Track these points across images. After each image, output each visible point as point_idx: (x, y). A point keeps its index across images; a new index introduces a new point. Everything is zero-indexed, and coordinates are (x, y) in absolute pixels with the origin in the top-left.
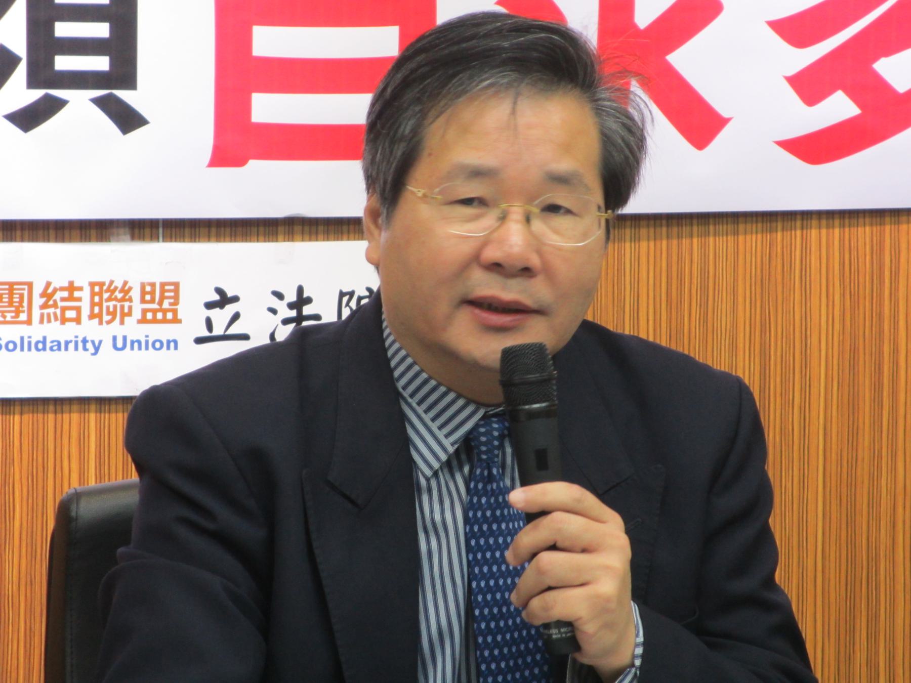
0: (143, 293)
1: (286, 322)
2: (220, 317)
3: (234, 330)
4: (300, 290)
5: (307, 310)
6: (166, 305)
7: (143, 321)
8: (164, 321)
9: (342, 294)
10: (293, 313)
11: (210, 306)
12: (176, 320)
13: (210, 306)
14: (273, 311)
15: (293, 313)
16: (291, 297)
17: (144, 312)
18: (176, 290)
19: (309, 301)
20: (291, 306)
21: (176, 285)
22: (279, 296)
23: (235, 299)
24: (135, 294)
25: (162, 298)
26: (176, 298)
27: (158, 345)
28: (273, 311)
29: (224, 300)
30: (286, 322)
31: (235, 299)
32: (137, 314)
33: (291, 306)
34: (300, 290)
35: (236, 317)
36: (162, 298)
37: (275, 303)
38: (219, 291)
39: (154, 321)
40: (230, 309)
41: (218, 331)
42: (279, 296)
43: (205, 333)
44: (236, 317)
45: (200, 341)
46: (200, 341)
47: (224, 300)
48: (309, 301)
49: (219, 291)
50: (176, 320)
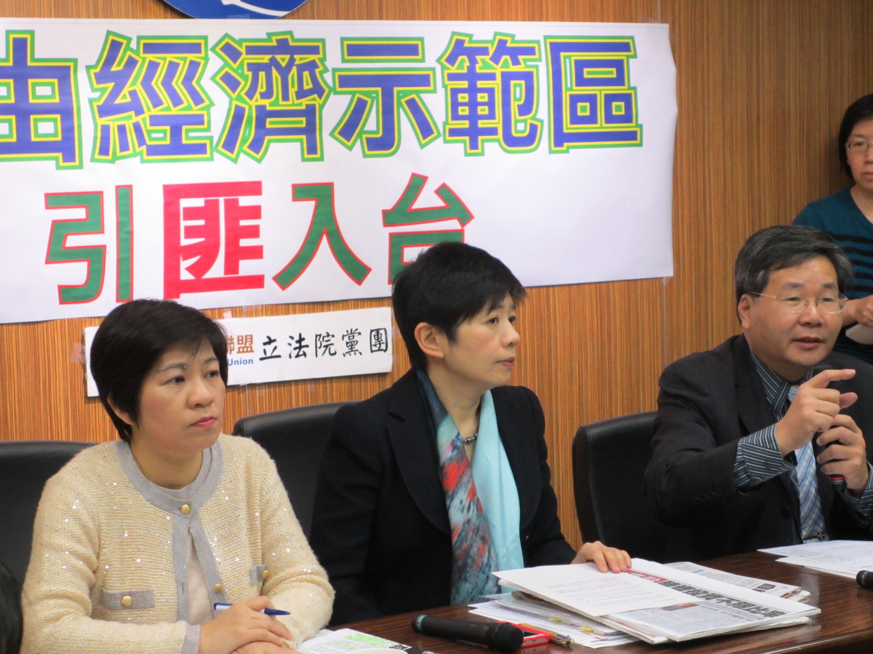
0: (239, 340)
1: (295, 349)
2: (269, 348)
3: (274, 354)
4: (300, 335)
5: (303, 343)
6: (248, 345)
7: (239, 352)
8: (247, 351)
9: (317, 336)
10: (298, 345)
11: (265, 344)
12: (252, 351)
13: (265, 344)
14: (290, 345)
15: (298, 345)
16: (297, 338)
17: (239, 348)
18: (251, 338)
19: (304, 339)
20: (297, 342)
21: (251, 336)
22: (292, 338)
23: (275, 340)
24: (235, 341)
25: (246, 342)
26: (252, 342)
27: (245, 362)
28: (290, 345)
29: (270, 341)
30: (295, 349)
31: (275, 340)
32: (236, 349)
33: (297, 342)
34: (300, 335)
35: (275, 348)
36: (246, 342)
37: (290, 341)
38: (269, 338)
39: (243, 352)
40: (273, 345)
41: (268, 354)
42: (292, 338)
43: (264, 356)
44: (275, 348)
45: (262, 359)
46: (262, 359)
47: (270, 341)
48: (304, 339)
49: (269, 338)
50: (252, 351)
